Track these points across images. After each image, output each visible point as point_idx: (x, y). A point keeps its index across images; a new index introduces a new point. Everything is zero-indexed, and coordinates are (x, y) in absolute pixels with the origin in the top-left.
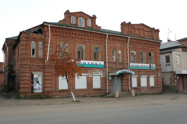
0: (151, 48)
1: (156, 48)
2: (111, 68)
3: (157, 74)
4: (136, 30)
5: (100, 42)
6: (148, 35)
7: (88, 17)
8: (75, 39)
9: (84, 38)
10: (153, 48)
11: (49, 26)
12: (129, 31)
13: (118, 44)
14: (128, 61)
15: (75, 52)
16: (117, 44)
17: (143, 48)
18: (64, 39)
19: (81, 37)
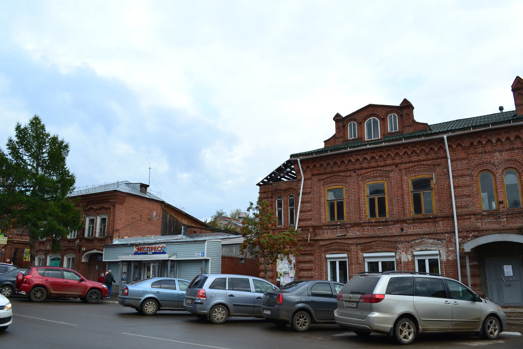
2: (474, 231)
5: (429, 162)
7: (390, 109)
8: (359, 172)
9: (382, 164)
11: (299, 160)
15: (362, 201)
16: (497, 154)
18: (336, 178)
19: (373, 164)
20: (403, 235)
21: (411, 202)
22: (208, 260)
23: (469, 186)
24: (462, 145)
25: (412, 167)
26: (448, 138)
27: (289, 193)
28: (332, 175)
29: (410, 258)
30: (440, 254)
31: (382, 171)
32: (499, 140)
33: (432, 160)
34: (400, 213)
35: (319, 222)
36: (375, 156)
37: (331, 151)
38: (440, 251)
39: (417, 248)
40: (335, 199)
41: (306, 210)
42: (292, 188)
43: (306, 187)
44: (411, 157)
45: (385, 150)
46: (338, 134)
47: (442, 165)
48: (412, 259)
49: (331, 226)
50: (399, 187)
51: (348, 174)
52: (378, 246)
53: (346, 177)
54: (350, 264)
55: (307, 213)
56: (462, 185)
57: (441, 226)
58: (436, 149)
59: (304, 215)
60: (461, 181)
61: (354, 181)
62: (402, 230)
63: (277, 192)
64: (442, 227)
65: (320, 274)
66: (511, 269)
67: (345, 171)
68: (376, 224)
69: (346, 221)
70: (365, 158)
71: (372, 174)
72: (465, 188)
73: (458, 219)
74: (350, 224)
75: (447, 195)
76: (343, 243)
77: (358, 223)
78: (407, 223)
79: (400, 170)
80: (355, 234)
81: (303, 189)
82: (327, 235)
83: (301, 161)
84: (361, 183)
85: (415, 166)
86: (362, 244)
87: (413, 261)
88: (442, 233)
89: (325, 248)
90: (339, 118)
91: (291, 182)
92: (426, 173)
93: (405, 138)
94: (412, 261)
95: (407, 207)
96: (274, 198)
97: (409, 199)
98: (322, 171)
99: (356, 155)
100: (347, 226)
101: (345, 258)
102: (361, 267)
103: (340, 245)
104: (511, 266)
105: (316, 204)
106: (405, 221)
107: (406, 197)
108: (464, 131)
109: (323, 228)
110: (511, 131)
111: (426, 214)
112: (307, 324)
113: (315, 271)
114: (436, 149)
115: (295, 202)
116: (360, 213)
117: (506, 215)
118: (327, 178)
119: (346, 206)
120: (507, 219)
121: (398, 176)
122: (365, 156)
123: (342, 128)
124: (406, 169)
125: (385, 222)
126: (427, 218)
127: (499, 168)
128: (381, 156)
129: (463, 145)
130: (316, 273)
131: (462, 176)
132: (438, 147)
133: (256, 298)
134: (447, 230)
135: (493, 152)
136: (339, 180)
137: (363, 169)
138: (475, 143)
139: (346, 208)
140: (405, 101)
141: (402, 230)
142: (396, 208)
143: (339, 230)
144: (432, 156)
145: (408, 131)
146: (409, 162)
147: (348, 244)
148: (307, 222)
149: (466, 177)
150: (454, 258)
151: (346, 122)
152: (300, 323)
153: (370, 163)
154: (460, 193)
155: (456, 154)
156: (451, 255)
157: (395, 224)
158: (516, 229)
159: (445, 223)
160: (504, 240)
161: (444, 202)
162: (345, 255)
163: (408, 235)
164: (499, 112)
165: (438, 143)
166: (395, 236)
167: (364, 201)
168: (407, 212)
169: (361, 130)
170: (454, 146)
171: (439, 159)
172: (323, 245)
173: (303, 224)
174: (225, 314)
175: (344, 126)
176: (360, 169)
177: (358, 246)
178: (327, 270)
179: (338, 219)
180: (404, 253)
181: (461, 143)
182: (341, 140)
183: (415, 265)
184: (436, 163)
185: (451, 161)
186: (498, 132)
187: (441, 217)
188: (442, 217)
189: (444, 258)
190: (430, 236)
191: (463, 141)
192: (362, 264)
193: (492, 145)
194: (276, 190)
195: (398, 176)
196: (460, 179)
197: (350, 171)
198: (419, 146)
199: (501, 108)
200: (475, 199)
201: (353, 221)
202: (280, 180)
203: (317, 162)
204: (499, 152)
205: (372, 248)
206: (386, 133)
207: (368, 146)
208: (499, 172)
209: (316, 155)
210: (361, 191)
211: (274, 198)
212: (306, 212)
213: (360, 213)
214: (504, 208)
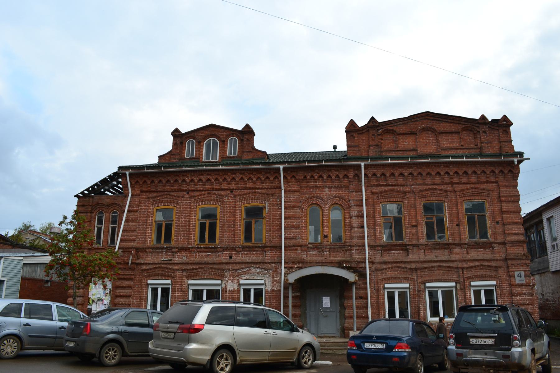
0: (473, 185)
1: (496, 182)
2: (299, 263)
3: (510, 276)
4: (401, 137)
5: (264, 191)
6: (456, 145)
7: (231, 132)
8: (193, 194)
9: (217, 187)
10: (485, 186)
11: (127, 173)
12: (369, 146)
13: (330, 188)
14: (363, 238)
15: (192, 225)
16: (327, 190)
17: (433, 189)
18: (167, 198)
19: (208, 187)
20: (231, 263)
21: (242, 229)
22: (3, 281)
23: (299, 218)
24: (296, 178)
25: (246, 194)
26: (284, 169)
27: (112, 209)
28: (163, 193)
29: (236, 287)
30: (265, 284)
31: (216, 194)
32: (329, 177)
33: (267, 189)
34: (230, 239)
35: (143, 244)
36: (211, 178)
37: (165, 167)
38: (266, 281)
39: (243, 277)
40: (163, 220)
41: (130, 230)
42: (116, 204)
43: (133, 204)
44: (246, 184)
45: (222, 173)
46: (175, 150)
47: (275, 195)
48: (238, 288)
49: (156, 249)
50: (231, 213)
51: (181, 194)
52: (205, 273)
53: (178, 197)
54: (173, 292)
55: (131, 233)
56: (292, 216)
57: (269, 256)
58: (272, 179)
59: (127, 235)
60: (292, 212)
61: (186, 202)
62: (231, 257)
63: (98, 207)
64: (270, 256)
65: (139, 301)
66: (329, 300)
67: (178, 191)
68: (205, 250)
69: (173, 244)
70: (200, 180)
71: (206, 197)
72: (295, 219)
73: (285, 250)
74: (177, 248)
75: (278, 225)
76: (167, 268)
77: (186, 248)
78: (236, 251)
79: (235, 196)
80: (181, 259)
81: (129, 205)
82: (151, 258)
83: (130, 174)
84: (193, 206)
85: (249, 193)
86: (188, 270)
87: (239, 290)
88: (269, 263)
89: (147, 273)
90: (177, 134)
91: (116, 197)
92: (260, 201)
93: (244, 164)
94: (238, 290)
95: (237, 234)
96: (94, 213)
97: (241, 226)
98: (153, 188)
99: (191, 175)
100: (174, 250)
101: (169, 284)
102: (184, 295)
103: (164, 271)
104: (329, 298)
105: (142, 224)
106: (234, 249)
107: (237, 224)
108: (299, 164)
109: (147, 250)
110: (340, 169)
111: (255, 243)
112: (117, 358)
113: (134, 298)
114: (272, 179)
115: (118, 220)
116: (189, 237)
117: (329, 249)
118: (158, 197)
119: (175, 229)
120: (329, 253)
121: (233, 201)
122: (200, 177)
123: (179, 144)
124: (240, 195)
125: (215, 248)
126: (256, 247)
127: (327, 203)
128: (217, 179)
129: (297, 177)
130: (135, 300)
131: (293, 207)
132: (274, 176)
133: (58, 328)
134: (275, 260)
135: (324, 187)
136: (170, 199)
137: (197, 191)
138: (308, 177)
139: (175, 230)
140: (247, 126)
141: (231, 257)
142: (227, 234)
143: (164, 254)
144: (267, 185)
145: (247, 157)
146: (244, 189)
147: (173, 270)
148: (130, 243)
149: (297, 209)
150: (278, 288)
151: (185, 139)
152: (109, 357)
153: (205, 185)
154: (290, 224)
155: (289, 185)
156: (276, 285)
157: (224, 251)
158: (337, 263)
159: (273, 253)
160: (325, 273)
161: (274, 232)
162: (169, 282)
163: (236, 263)
164: (333, 150)
165: (274, 172)
166: (223, 263)
167: (194, 225)
168: (237, 239)
169: (200, 149)
170: (289, 178)
171: (273, 188)
172: (145, 270)
173: (125, 245)
174: (17, 347)
175: (182, 143)
176: (194, 191)
177: (184, 272)
178: (147, 298)
179: (165, 242)
180: (230, 281)
181: (295, 175)
182: (177, 157)
183: (240, 294)
184: (270, 192)
185: (284, 192)
186: (330, 169)
187: (270, 247)
188: (271, 247)
189: (269, 288)
190: (258, 266)
191: (297, 174)
192: (186, 292)
193: (323, 181)
194: (98, 204)
195: (233, 201)
196: (291, 210)
197: (184, 191)
198: (255, 173)
199: (335, 147)
200: (303, 231)
201: (181, 245)
202: (103, 193)
203: (148, 178)
204: (328, 188)
205: (198, 275)
206: (225, 156)
207: (205, 167)
208: (327, 207)
209: (148, 170)
210: (193, 213)
211: (94, 213)
212: (130, 232)
213: (189, 238)
214: (328, 241)
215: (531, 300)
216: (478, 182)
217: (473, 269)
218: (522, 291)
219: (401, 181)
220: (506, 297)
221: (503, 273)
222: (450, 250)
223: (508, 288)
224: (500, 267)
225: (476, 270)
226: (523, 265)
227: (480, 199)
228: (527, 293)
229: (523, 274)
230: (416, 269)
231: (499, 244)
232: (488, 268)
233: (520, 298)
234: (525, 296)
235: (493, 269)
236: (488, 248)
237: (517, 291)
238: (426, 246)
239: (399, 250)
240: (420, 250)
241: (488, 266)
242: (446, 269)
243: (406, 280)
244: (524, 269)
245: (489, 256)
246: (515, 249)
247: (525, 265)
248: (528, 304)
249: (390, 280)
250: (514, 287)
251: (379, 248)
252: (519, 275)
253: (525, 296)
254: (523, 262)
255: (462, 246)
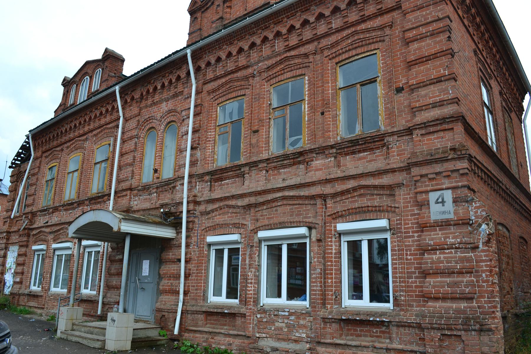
0: (353, 29)
7: (95, 64)
104: (149, 261)
117: (157, 188)
215: (469, 260)
216: (363, 20)
217: (346, 197)
218: (445, 238)
219: (242, 61)
220: (411, 255)
221: (407, 198)
222: (307, 163)
223: (416, 235)
224: (400, 185)
225: (352, 197)
226: (450, 173)
227: (368, 51)
228: (460, 243)
229: (448, 195)
230: (249, 206)
231: (399, 134)
232: (375, 192)
233: (442, 256)
234: (456, 253)
235: (385, 192)
236: (378, 148)
237: (432, 239)
238: (268, 164)
239: (233, 177)
240: (261, 171)
241: (375, 187)
242: (296, 202)
243: (237, 227)
244: (454, 184)
245: (380, 164)
246: (435, 139)
247: (455, 174)
248: (460, 273)
249: (214, 229)
250: (427, 231)
251: (207, 178)
252: (440, 200)
253: (456, 253)
254: (450, 166)
255: (327, 152)
